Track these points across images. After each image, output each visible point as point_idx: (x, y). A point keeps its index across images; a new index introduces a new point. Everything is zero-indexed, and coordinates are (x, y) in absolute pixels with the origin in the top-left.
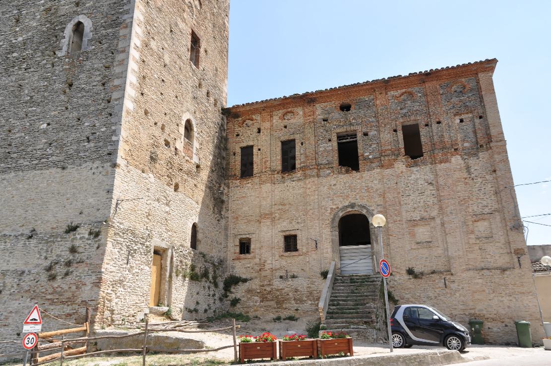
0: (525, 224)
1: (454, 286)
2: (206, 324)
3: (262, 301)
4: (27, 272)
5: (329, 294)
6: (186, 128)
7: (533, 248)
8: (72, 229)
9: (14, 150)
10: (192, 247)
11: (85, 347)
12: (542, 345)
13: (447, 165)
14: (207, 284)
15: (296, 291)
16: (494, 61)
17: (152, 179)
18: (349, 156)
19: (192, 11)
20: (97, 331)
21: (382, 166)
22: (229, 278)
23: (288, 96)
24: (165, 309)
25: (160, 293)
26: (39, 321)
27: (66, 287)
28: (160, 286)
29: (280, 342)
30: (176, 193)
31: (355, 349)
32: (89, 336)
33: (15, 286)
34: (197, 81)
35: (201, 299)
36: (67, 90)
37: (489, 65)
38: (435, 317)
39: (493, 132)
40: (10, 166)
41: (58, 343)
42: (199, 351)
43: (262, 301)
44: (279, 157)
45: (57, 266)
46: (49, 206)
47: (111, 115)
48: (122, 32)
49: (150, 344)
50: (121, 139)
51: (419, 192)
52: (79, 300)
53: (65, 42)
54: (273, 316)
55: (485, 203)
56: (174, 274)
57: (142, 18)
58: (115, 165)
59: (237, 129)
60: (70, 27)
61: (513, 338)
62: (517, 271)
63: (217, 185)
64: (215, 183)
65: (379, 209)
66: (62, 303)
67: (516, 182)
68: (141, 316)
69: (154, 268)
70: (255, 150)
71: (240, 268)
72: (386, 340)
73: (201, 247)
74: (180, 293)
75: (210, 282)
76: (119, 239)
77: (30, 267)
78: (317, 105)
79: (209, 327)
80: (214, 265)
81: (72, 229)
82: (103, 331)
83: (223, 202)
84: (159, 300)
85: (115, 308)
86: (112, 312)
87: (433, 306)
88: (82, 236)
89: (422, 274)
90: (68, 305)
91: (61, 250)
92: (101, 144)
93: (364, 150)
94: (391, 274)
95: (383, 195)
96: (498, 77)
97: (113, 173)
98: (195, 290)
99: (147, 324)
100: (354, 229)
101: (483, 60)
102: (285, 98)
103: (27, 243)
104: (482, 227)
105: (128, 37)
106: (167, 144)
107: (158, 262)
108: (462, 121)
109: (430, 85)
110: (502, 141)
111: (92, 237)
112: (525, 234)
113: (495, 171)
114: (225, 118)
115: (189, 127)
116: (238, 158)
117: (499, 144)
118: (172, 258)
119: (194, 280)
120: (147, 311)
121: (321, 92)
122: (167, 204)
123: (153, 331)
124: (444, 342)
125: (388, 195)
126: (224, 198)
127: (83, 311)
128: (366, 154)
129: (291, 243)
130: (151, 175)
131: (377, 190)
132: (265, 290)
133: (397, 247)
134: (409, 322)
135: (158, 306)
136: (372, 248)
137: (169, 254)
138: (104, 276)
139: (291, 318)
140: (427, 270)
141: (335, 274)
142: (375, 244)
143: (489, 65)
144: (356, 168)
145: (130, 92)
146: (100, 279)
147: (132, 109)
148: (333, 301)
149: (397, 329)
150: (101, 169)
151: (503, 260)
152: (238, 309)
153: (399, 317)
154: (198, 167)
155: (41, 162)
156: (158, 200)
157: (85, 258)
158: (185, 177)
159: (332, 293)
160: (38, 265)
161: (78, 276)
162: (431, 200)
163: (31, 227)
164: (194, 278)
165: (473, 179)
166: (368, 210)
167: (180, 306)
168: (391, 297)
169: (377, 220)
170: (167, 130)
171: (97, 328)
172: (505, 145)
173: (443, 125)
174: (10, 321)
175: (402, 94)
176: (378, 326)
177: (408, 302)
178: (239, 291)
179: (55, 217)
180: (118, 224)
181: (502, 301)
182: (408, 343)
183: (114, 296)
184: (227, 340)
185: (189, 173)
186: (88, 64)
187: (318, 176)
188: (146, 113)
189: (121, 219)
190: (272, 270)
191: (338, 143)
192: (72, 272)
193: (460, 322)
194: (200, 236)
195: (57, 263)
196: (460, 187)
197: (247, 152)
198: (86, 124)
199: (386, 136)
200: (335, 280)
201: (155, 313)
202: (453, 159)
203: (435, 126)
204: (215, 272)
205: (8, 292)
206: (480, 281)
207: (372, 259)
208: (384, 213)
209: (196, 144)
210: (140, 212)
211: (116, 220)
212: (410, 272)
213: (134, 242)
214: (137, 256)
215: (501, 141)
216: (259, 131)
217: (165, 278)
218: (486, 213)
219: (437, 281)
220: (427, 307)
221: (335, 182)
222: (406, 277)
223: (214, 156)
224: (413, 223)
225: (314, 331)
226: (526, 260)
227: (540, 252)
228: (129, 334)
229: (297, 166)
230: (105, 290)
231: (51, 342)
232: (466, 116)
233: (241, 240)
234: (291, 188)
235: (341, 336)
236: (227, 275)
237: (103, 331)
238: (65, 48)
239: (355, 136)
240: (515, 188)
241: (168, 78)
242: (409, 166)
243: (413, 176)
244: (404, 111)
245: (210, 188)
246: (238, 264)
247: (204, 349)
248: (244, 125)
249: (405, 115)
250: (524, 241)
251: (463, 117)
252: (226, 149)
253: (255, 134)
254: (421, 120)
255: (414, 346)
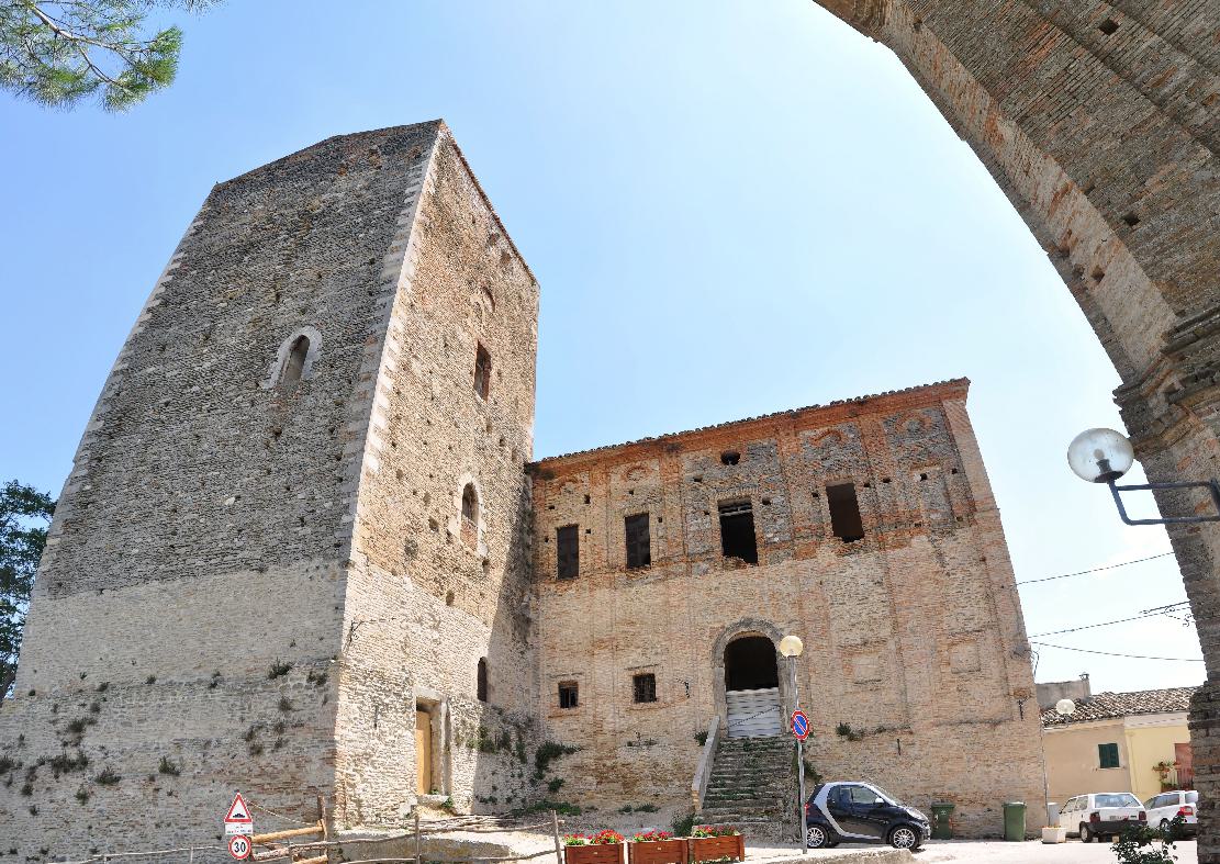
0: (1034, 648)
1: (913, 752)
2: (507, 822)
3: (599, 783)
4: (214, 743)
5: (709, 770)
6: (465, 498)
7: (1045, 688)
8: (281, 671)
9: (182, 541)
10: (479, 697)
11: (325, 856)
12: (1039, 837)
13: (906, 549)
14: (507, 760)
15: (656, 765)
16: (965, 382)
17: (410, 586)
18: (739, 540)
19: (479, 316)
20: (340, 833)
21: (795, 556)
22: (544, 747)
23: (634, 441)
24: (444, 799)
25: (432, 772)
26: (246, 818)
27: (281, 767)
28: (431, 761)
29: (629, 844)
30: (449, 608)
31: (748, 851)
32: (328, 840)
33: (200, 765)
34: (484, 421)
35: (500, 780)
36: (272, 442)
37: (958, 388)
38: (879, 800)
39: (977, 494)
40: (173, 568)
41: (283, 851)
42: (502, 860)
43: (599, 783)
44: (623, 544)
45: (262, 733)
46: (241, 634)
47: (341, 480)
48: (367, 350)
49: (424, 851)
50: (357, 519)
51: (860, 597)
52: (304, 787)
53: (275, 369)
54: (616, 804)
55: (968, 614)
56: (452, 743)
57: (401, 329)
58: (346, 564)
59: (552, 498)
60: (287, 344)
61: (998, 829)
62: (1014, 725)
63: (519, 593)
64: (514, 589)
65: (793, 626)
66: (279, 790)
67: (1019, 577)
68: (404, 810)
69: (420, 733)
70: (581, 532)
71: (561, 730)
72: (798, 837)
73: (495, 698)
74: (465, 772)
75: (513, 755)
76: (359, 687)
77: (218, 733)
78: (683, 456)
79: (515, 823)
80: (519, 727)
81: (281, 671)
82: (349, 832)
83: (528, 621)
84: (432, 784)
85: (362, 797)
86: (359, 803)
87: (877, 783)
88: (297, 682)
89: (862, 733)
90: (288, 794)
91: (265, 707)
92: (323, 529)
93: (766, 529)
94: (811, 735)
95: (799, 604)
96: (974, 405)
97: (344, 577)
98: (488, 769)
99: (417, 821)
100: (750, 663)
101: (947, 380)
102: (630, 445)
103: (210, 695)
104: (964, 654)
105: (376, 358)
106: (434, 525)
107: (426, 723)
108: (924, 477)
109: (867, 421)
110: (995, 509)
111: (314, 683)
112: (1035, 664)
113: (984, 560)
114: (529, 479)
115: (469, 497)
116: (553, 545)
117: (991, 514)
118: (448, 716)
119: (487, 752)
120: (415, 802)
121: (688, 434)
122: (435, 628)
123: (426, 831)
124: (888, 839)
125: (806, 603)
126: (532, 615)
127: (312, 802)
128: (770, 535)
129: (644, 688)
130: (407, 580)
131: (789, 595)
132: (604, 765)
133: (821, 687)
134: (835, 808)
135: (431, 793)
136: (781, 690)
137: (444, 711)
138: (340, 748)
139: (648, 809)
140: (871, 726)
141: (718, 737)
142: (785, 687)
143: (958, 388)
144: (752, 558)
145: (374, 442)
146: (334, 752)
147: (376, 469)
148: (715, 781)
149: (815, 819)
150: (322, 571)
151: (995, 707)
152: (562, 796)
153: (821, 802)
154: (486, 563)
155: (223, 561)
156: (420, 621)
157: (305, 718)
158: (464, 580)
159: (714, 768)
160: (229, 732)
161: (297, 748)
162: (884, 611)
163: (212, 669)
164: (486, 748)
165: (948, 574)
166: (775, 632)
167: (467, 793)
168: (810, 773)
169: (789, 646)
170: (433, 505)
171: (339, 827)
172: (998, 517)
173: (894, 483)
174: (201, 817)
175: (824, 435)
176: (786, 816)
177: (834, 780)
178: (561, 768)
179: (252, 650)
180: (356, 663)
181: (988, 773)
182: (832, 841)
183: (358, 778)
184: (547, 842)
185: (470, 574)
186: (309, 401)
187: (688, 573)
188: (399, 475)
189: (362, 654)
190: (614, 733)
191: (723, 520)
192: (287, 741)
193: (920, 807)
194: (492, 679)
195: (260, 728)
196: (929, 587)
197: (568, 536)
198: (300, 496)
199: (802, 504)
200: (718, 747)
201: (427, 805)
202: (914, 541)
203: (880, 487)
204: (520, 739)
205: (191, 774)
206: (956, 742)
207: (781, 711)
208: (803, 633)
209: (482, 525)
210: (390, 641)
211: (351, 656)
212: (843, 730)
213: (383, 692)
214: (391, 715)
215: (991, 509)
216: (588, 500)
217: (438, 750)
218: (970, 630)
219: (886, 744)
220: (866, 785)
221: (715, 584)
222: (836, 739)
223: (513, 544)
224: (849, 651)
225: (683, 827)
226: (1031, 707)
227: (1057, 694)
228: (392, 837)
229: (654, 558)
230: (343, 770)
231: (272, 848)
232: (932, 469)
233: (560, 685)
234: (645, 594)
235: (728, 832)
236: (540, 742)
237: (349, 832)
238: (275, 377)
239: (748, 505)
240: (1018, 588)
241: (436, 417)
242: (841, 554)
243: (849, 571)
244: (827, 464)
245: (507, 598)
246: (557, 725)
247: (511, 856)
248: (562, 490)
249: (829, 469)
250: (1031, 675)
251: (925, 470)
252: (532, 531)
253: (581, 504)
254: (859, 477)
255: (841, 845)
